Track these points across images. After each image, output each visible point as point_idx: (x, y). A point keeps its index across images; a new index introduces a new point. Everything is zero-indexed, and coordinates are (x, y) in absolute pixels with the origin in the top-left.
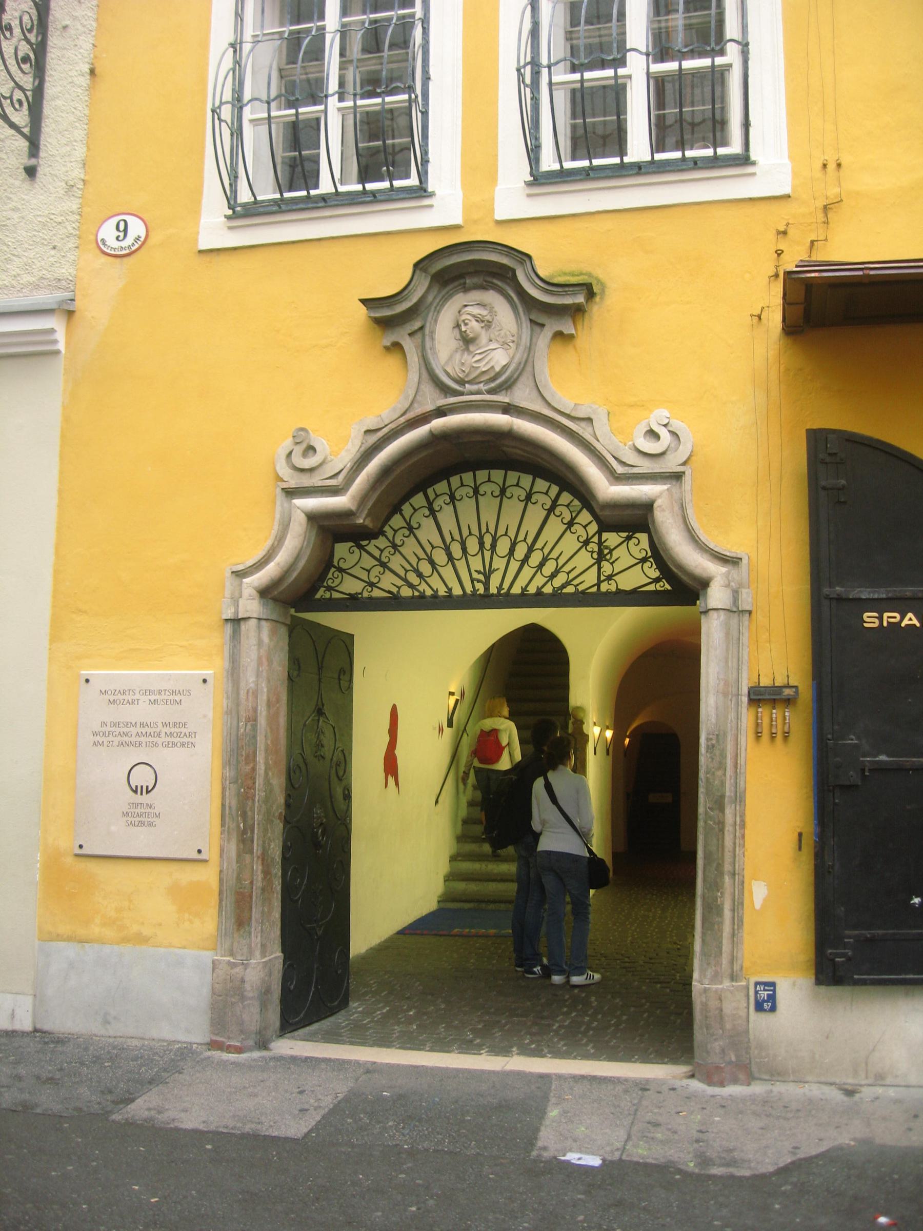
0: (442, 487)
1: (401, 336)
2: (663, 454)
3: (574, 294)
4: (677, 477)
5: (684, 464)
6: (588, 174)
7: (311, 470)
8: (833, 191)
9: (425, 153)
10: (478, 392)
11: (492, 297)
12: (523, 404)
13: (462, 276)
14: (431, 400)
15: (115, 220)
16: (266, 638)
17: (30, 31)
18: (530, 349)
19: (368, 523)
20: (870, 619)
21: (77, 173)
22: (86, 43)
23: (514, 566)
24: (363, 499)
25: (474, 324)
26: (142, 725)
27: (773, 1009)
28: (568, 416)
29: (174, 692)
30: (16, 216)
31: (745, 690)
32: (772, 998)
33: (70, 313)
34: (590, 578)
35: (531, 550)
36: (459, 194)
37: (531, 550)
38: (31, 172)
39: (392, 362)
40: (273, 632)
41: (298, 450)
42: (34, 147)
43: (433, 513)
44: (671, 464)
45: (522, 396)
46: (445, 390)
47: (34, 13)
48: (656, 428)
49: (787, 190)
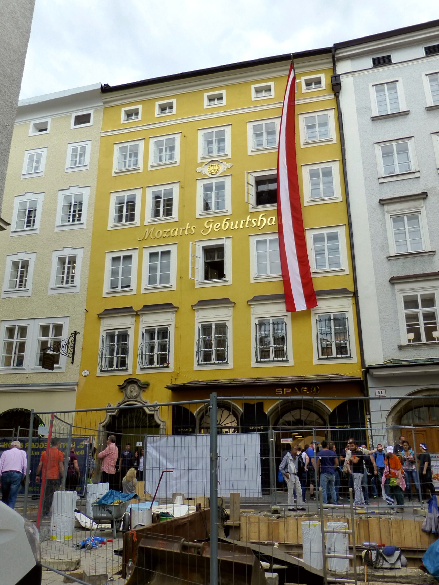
1: (123, 390)
6: (148, 368)
9: (127, 363)
11: (135, 385)
14: (127, 399)
18: (140, 393)
25: (132, 389)
36: (132, 370)
38: (72, 363)
39: (122, 394)
41: (109, 406)
45: (138, 399)
46: (129, 398)
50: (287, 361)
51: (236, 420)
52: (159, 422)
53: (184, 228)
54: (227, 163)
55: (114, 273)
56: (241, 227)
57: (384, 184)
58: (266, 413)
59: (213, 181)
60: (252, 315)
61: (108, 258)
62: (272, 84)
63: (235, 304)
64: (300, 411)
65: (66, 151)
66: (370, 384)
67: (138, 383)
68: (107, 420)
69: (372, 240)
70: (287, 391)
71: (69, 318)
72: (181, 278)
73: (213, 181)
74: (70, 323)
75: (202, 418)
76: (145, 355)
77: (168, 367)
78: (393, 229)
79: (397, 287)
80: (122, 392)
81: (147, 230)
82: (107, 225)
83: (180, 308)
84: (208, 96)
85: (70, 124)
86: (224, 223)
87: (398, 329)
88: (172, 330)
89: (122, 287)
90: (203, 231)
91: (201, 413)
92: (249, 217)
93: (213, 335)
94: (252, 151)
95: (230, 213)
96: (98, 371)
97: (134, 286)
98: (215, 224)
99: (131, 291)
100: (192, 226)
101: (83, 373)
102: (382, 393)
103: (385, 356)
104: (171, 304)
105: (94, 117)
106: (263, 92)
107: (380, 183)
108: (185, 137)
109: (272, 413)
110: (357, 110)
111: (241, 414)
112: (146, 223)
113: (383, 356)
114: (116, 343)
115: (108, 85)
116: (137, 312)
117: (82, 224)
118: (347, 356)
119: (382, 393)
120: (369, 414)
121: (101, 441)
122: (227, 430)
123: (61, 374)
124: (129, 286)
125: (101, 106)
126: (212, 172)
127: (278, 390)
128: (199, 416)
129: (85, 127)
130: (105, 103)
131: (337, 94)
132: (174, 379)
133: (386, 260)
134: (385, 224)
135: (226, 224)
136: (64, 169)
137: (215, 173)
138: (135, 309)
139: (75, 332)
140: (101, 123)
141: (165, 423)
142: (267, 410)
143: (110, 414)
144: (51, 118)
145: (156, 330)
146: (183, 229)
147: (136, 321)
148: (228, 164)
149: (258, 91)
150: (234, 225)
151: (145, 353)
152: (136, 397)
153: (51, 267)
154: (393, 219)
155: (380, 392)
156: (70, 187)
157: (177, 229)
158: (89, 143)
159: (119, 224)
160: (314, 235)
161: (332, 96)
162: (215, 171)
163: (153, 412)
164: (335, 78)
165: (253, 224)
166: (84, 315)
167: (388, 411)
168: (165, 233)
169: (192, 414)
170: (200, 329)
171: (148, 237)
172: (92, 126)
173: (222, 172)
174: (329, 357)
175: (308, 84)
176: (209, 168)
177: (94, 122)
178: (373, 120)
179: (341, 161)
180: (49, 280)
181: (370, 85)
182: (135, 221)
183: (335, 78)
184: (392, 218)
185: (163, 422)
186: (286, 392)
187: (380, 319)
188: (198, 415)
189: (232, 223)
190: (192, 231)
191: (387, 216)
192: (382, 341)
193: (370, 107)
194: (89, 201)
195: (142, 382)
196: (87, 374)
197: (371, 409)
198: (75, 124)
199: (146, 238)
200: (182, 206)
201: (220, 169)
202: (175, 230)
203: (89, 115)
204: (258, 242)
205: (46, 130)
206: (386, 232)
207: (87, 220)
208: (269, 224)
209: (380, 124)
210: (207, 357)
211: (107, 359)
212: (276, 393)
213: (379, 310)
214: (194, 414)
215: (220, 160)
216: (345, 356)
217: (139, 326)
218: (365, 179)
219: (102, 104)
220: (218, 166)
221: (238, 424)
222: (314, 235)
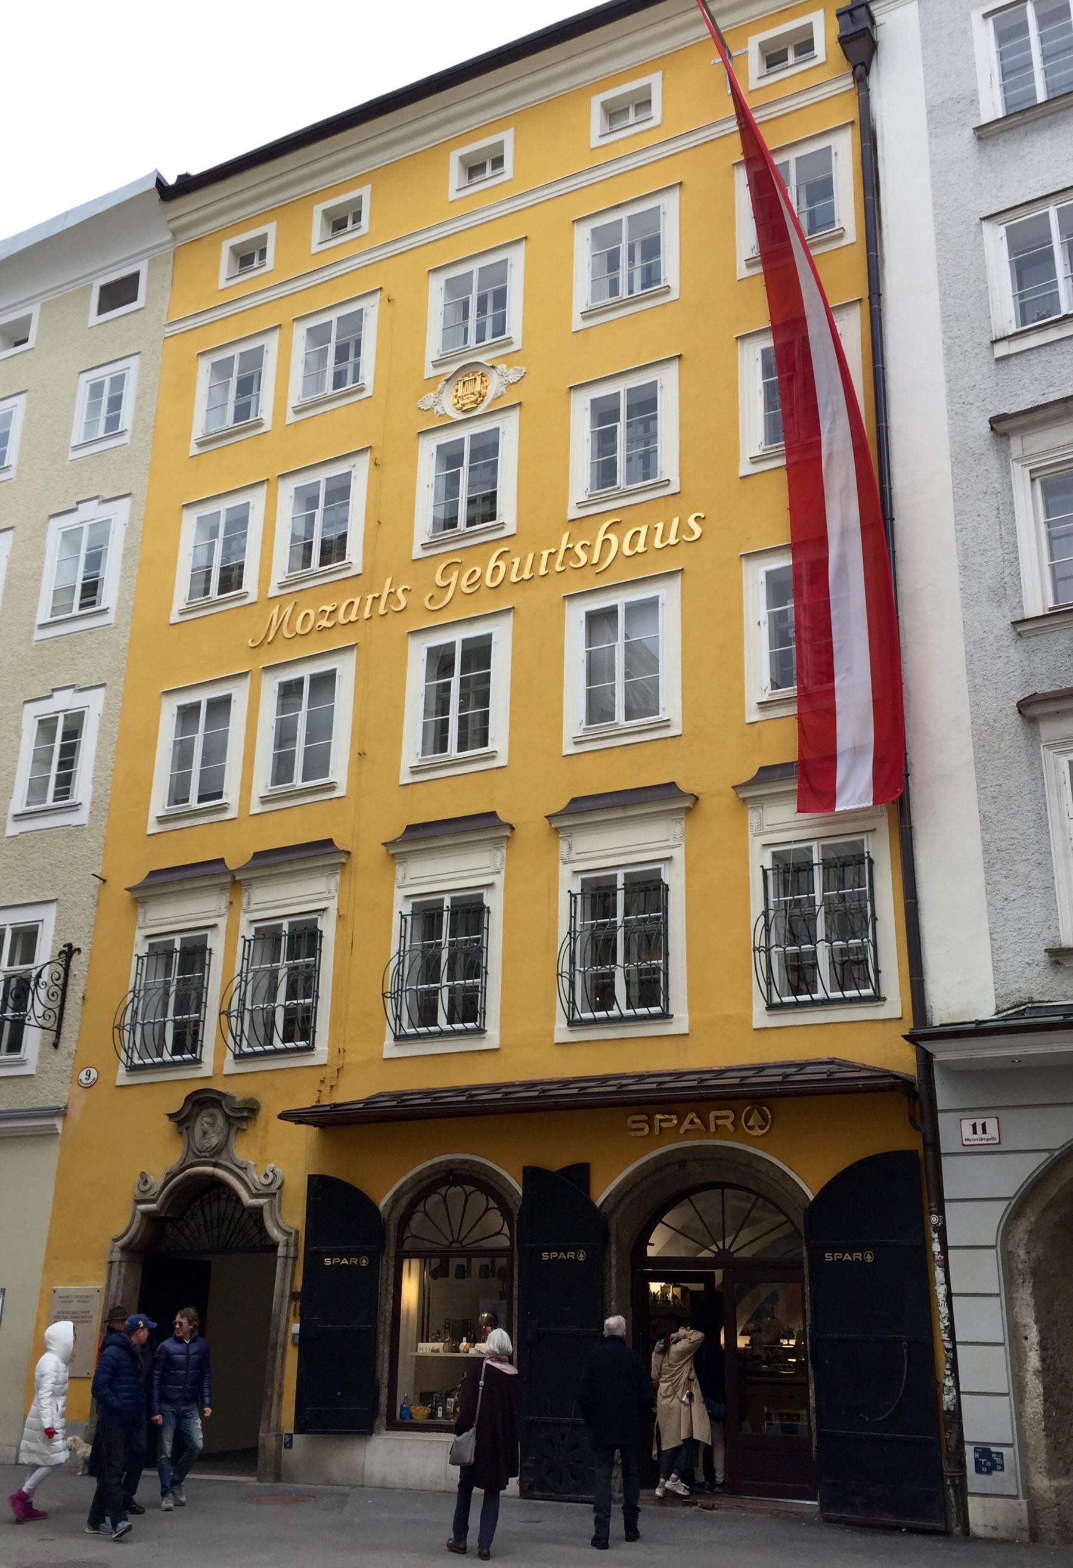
0: (206, 1196)
2: (271, 1184)
3: (242, 1112)
4: (274, 1194)
5: (279, 1188)
7: (146, 1191)
8: (341, 1063)
10: (206, 1157)
11: (216, 1112)
12: (222, 1162)
13: (205, 1102)
14: (191, 1160)
15: (85, 1070)
16: (123, 1270)
17: (58, 980)
18: (228, 1136)
19: (168, 1215)
20: (328, 1261)
21: (74, 1047)
22: (83, 982)
23: (230, 1233)
24: (162, 1206)
25: (206, 1125)
26: (74, 1313)
27: (291, 1447)
28: (240, 1168)
29: (87, 1297)
30: (49, 1066)
31: (288, 1293)
32: (291, 1441)
33: (65, 1115)
34: (257, 1239)
35: (236, 1226)
37: (236, 1226)
38: (56, 1045)
40: (127, 1269)
41: (142, 1181)
42: (58, 1033)
43: (203, 1211)
44: (273, 1189)
47: (61, 970)
48: (268, 1173)
49: (325, 1062)
50: (665, 1016)
51: (506, 1227)
52: (275, 1233)
53: (377, 595)
54: (509, 366)
55: (183, 756)
56: (542, 572)
57: (1013, 360)
58: (598, 1203)
59: (465, 433)
60: (565, 863)
61: (169, 711)
62: (655, 80)
63: (512, 828)
64: (723, 1192)
65: (73, 395)
66: (943, 1099)
67: (223, 1104)
68: (135, 1226)
69: (964, 568)
70: (664, 1125)
71: (55, 904)
72: (361, 754)
73: (465, 433)
74: (58, 920)
75: (404, 1221)
76: (252, 1011)
77: (310, 1048)
78: (1042, 519)
79: (1048, 730)
80: (181, 1133)
81: (275, 612)
82: (170, 609)
83: (353, 854)
84: (462, 159)
85: (87, 312)
86: (492, 565)
87: (1049, 889)
88: (327, 926)
89: (201, 799)
90: (432, 596)
91: (404, 1202)
92: (566, 536)
93: (445, 939)
94: (586, 315)
95: (510, 530)
96: (122, 1070)
97: (231, 794)
98: (466, 571)
99: (223, 808)
100: (398, 585)
101: (83, 1076)
102: (984, 1132)
103: (1002, 991)
104: (329, 842)
105: (150, 280)
106: (632, 112)
107: (998, 360)
108: (389, 301)
109: (618, 1203)
110: (929, 113)
111: (519, 1203)
112: (273, 591)
113: (993, 992)
114: (175, 976)
115: (187, 175)
116: (232, 873)
117: (104, 611)
118: (865, 992)
119: (984, 1132)
120: (941, 1212)
121: (116, 1297)
122: (463, 1261)
123: (25, 1083)
124: (219, 795)
125: (167, 243)
126: (463, 405)
127: (633, 1122)
128: (395, 1215)
129: (125, 315)
130: (175, 233)
131: (859, 69)
132: (326, 1089)
133: (1011, 635)
134: (1012, 504)
135: (497, 567)
136: (67, 452)
137: (475, 405)
138: (232, 864)
139: (70, 946)
140: (167, 298)
141: (292, 1240)
142: (601, 1193)
143: (142, 1207)
144: (39, 303)
145: (286, 928)
146: (374, 598)
147: (231, 903)
148: (511, 371)
149: (614, 113)
150: (520, 569)
151: (252, 1005)
152: (218, 1151)
153: (18, 752)
154: (1042, 483)
155: (979, 1129)
156: (78, 503)
157: (357, 601)
158: (134, 362)
159: (199, 600)
160: (769, 574)
161: (848, 83)
162: (473, 398)
163: (262, 1201)
164: (852, 15)
165: (579, 559)
166: (94, 892)
167: (1007, 1202)
168: (323, 618)
169: (372, 1206)
170: (409, 918)
171: (277, 632)
172: (142, 309)
173: (495, 399)
174: (848, 994)
175: (774, 58)
176: (457, 391)
177: (148, 296)
178: (980, 138)
179: (866, 302)
180: (12, 790)
181: (976, 16)
182: (244, 589)
183: (852, 15)
184: (1038, 483)
185: (289, 1234)
186: (716, 1125)
187: (986, 852)
188: (392, 1209)
189: (517, 561)
190: (399, 602)
191: (1020, 475)
192: (991, 933)
193: (975, 92)
194: (125, 541)
195: (238, 1099)
196: (92, 1078)
197: (949, 1190)
198: (101, 311)
199: (270, 639)
200: (375, 524)
201: (488, 391)
202: (352, 603)
203: (133, 279)
204: (593, 618)
205: (25, 341)
206: (1013, 532)
207: (119, 599)
208: (627, 552)
209: (1004, 150)
210: (427, 1013)
211: (148, 1029)
212: (632, 1134)
213: (984, 818)
214: (382, 1204)
215: (487, 361)
216: (807, 997)
217: (239, 917)
218: (948, 353)
219: (169, 237)
220: (482, 382)
221: (511, 1239)
222: (769, 574)
